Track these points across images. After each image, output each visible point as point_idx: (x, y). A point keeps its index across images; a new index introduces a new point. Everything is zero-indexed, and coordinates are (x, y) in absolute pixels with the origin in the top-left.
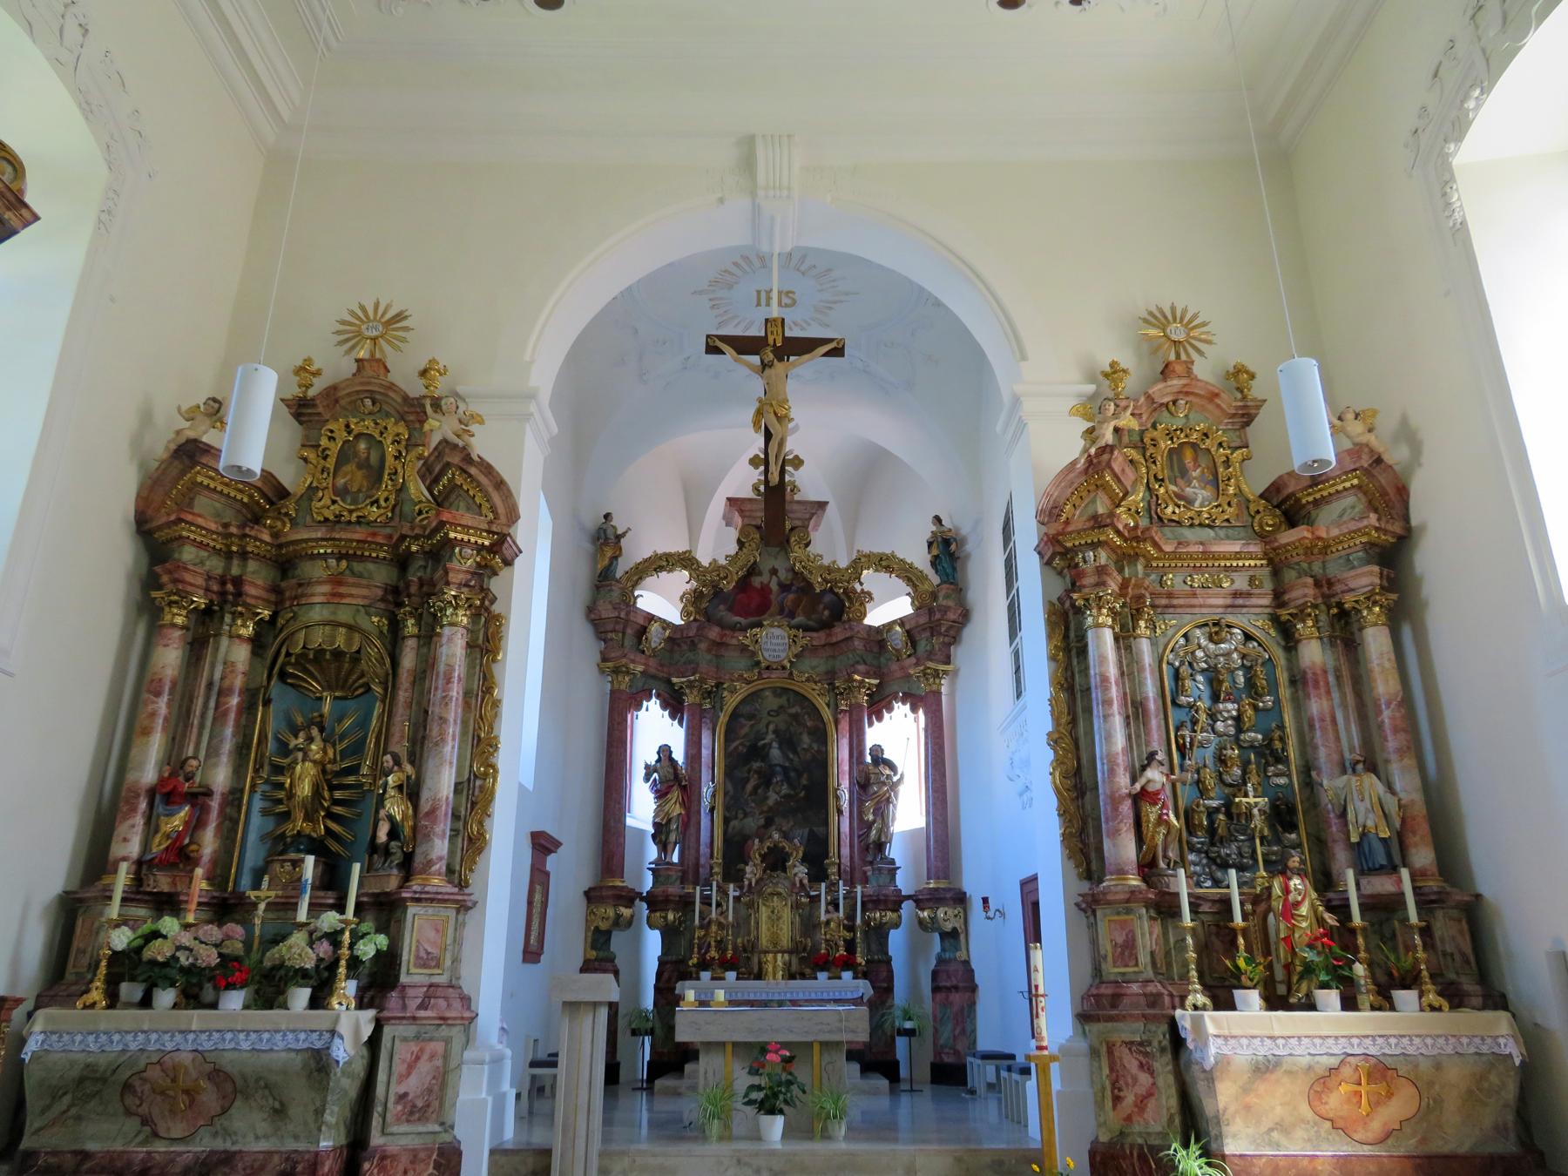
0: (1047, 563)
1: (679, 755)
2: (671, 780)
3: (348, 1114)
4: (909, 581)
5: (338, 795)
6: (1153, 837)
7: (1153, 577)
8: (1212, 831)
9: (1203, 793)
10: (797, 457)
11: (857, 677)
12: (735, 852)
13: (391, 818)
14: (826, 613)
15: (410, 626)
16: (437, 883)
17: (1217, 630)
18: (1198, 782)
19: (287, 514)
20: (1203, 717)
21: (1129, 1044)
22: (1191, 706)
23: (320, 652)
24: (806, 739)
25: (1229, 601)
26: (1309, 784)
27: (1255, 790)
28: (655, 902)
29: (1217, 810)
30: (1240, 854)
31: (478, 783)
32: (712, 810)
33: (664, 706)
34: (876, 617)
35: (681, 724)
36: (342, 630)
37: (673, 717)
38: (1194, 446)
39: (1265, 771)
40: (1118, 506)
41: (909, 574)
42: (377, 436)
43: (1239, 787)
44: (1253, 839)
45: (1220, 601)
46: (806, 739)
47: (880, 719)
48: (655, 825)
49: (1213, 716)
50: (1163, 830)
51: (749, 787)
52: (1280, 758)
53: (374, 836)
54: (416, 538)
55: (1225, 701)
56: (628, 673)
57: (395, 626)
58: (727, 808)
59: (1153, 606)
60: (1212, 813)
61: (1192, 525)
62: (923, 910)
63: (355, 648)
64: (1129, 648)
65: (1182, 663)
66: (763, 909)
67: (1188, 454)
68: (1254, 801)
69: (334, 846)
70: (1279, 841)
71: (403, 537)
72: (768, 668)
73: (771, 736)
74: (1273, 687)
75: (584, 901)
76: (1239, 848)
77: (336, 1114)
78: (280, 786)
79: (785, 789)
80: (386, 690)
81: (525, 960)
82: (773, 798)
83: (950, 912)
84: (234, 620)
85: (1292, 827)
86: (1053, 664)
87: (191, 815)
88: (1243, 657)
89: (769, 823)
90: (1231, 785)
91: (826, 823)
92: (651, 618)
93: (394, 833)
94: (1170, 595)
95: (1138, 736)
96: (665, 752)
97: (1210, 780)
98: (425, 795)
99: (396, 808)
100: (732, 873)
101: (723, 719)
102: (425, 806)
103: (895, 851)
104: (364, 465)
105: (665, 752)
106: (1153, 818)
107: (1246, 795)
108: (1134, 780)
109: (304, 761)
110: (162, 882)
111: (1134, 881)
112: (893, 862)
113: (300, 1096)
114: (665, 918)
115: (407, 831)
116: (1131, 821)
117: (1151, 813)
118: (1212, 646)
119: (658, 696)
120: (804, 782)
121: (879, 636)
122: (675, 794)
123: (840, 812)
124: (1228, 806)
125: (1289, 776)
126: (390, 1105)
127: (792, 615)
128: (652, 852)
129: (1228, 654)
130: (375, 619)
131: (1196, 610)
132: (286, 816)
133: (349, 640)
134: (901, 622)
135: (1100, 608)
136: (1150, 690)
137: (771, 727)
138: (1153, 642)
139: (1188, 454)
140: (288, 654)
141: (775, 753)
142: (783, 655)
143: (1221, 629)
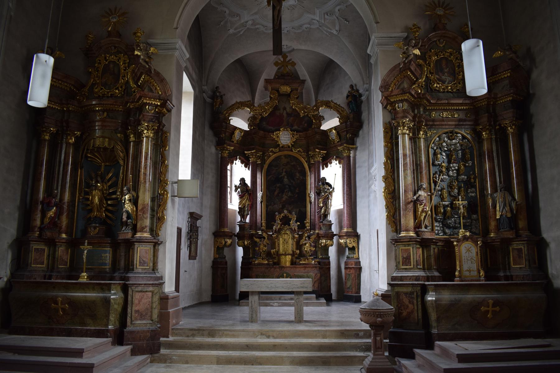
0: (385, 108)
1: (248, 182)
2: (245, 191)
3: (118, 316)
4: (338, 112)
6: (420, 217)
7: (427, 113)
8: (445, 213)
9: (442, 199)
10: (293, 62)
11: (317, 150)
12: (270, 218)
13: (127, 212)
14: (306, 125)
15: (132, 138)
16: (146, 235)
17: (451, 135)
18: (441, 194)
19: (84, 94)
20: (444, 170)
22: (440, 165)
23: (99, 148)
24: (298, 174)
25: (457, 123)
26: (483, 195)
27: (462, 198)
28: (240, 236)
29: (447, 206)
30: (455, 223)
31: (161, 197)
32: (261, 202)
33: (242, 162)
34: (325, 127)
35: (249, 169)
36: (107, 140)
37: (246, 166)
38: (446, 59)
39: (467, 191)
40: (414, 84)
41: (337, 109)
43: (456, 198)
44: (460, 217)
45: (454, 123)
46: (298, 174)
47: (327, 166)
48: (239, 208)
49: (448, 169)
50: (424, 214)
51: (276, 193)
52: (474, 186)
53: (122, 219)
54: (132, 102)
55: (453, 163)
56: (227, 150)
57: (127, 137)
58: (267, 201)
59: (426, 125)
60: (445, 207)
61: (444, 92)
63: (112, 146)
64: (415, 142)
65: (437, 148)
66: (281, 239)
67: (444, 62)
68: (461, 203)
69: (109, 221)
70: (469, 217)
71: (127, 103)
72: (282, 147)
73: (284, 174)
74: (472, 159)
75: (213, 237)
76: (455, 220)
77: (113, 318)
78: (88, 199)
79: (290, 194)
80: (124, 164)
81: (189, 259)
82: (285, 197)
83: (352, 240)
84: (67, 137)
85: (476, 212)
86: (386, 149)
87: (56, 210)
88: (461, 145)
89: (283, 208)
90: (453, 196)
91: (305, 207)
92: (235, 128)
93: (129, 217)
94: (434, 120)
95: (417, 177)
96: (243, 180)
97: (445, 195)
98: (140, 202)
99: (128, 207)
100: (269, 226)
101: (266, 166)
102: (140, 207)
103: (332, 217)
105: (243, 180)
106: (420, 210)
107: (459, 201)
108: (415, 194)
109: (95, 190)
110: (48, 234)
111: (412, 234)
112: (330, 221)
114: (244, 243)
115: (134, 216)
116: (412, 211)
118: (449, 141)
119: (240, 159)
120: (297, 191)
121: (325, 133)
122: (247, 196)
123: (311, 203)
124: (452, 205)
125: (476, 193)
126: (133, 314)
127: (292, 126)
128: (239, 218)
129: (455, 144)
130: (119, 135)
131: (444, 127)
132: (91, 211)
133: (109, 144)
134: (335, 128)
135: (404, 127)
137: (284, 170)
138: (426, 140)
139: (444, 62)
140: (88, 149)
141: (286, 180)
142: (288, 142)
143: (453, 134)
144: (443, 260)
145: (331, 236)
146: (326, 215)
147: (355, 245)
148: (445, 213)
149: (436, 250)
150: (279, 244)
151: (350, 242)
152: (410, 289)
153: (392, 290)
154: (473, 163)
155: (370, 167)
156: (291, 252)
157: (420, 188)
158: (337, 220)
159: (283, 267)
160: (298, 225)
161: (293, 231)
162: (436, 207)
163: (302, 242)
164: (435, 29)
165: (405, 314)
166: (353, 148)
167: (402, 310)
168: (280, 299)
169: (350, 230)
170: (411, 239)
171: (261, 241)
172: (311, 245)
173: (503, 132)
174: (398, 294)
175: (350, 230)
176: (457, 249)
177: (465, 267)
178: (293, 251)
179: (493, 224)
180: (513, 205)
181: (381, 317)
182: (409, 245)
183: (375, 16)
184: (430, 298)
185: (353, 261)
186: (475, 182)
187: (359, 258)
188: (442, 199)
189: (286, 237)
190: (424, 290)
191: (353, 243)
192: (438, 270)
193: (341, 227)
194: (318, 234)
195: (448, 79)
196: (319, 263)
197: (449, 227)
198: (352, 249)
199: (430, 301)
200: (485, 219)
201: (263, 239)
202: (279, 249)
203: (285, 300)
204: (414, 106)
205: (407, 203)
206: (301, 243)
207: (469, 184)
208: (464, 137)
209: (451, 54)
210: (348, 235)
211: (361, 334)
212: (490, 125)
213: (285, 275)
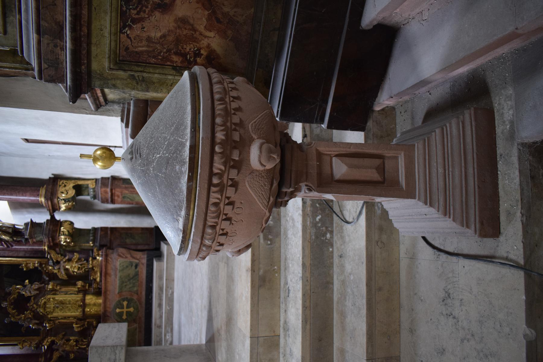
62: (60, 208)
66: (55, 314)
83: (62, 189)
103: (19, 220)
112: (26, 224)
145: (54, 224)
146: (14, 231)
147: (72, 185)
150: (65, 318)
151: (65, 193)
156: (80, 296)
158: (30, 210)
159: (105, 311)
160: (31, 283)
161: (42, 292)
163: (62, 275)
167: (197, 54)
168: (160, 327)
169: (43, 191)
171: (57, 350)
172: (69, 260)
175: (43, 191)
178: (79, 292)
181: (243, 145)
185: (100, 191)
187: (96, 180)
189: (50, 306)
191: (67, 188)
193: (36, 206)
194: (49, 247)
196: (101, 247)
198: (79, 189)
201: (54, 347)
202: (75, 317)
203: (161, 317)
206: (65, 277)
210: (51, 196)
213: (118, 310)
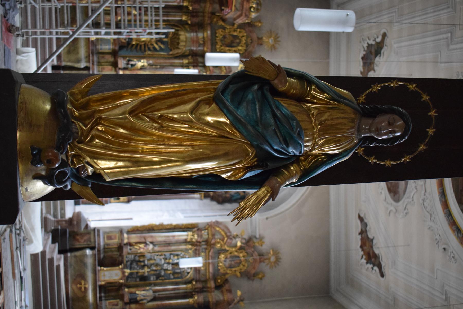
5: (143, 46)
20: (167, 261)
21: (90, 238)
22: (170, 259)
23: (179, 39)
26: (150, 285)
29: (144, 263)
42: (241, 44)
60: (144, 261)
70: (138, 277)
74: (175, 278)
77: (69, 64)
93: (132, 65)
97: (152, 262)
104: (232, 42)
111: (126, 241)
113: (73, 57)
117: (142, 246)
133: (181, 46)
136: (173, 248)
140: (178, 30)
144: (110, 258)
148: (140, 261)
149: (116, 256)
152: (92, 240)
153: (91, 230)
154: (172, 279)
155: (183, 211)
157: (154, 245)
162: (144, 256)
164: (261, 255)
165: (78, 237)
166: (201, 196)
170: (122, 240)
173: (191, 296)
174: (89, 233)
176: (117, 268)
177: (107, 273)
179: (133, 290)
180: (145, 301)
182: (119, 239)
183: (272, 217)
184: (88, 252)
186: (160, 280)
188: (149, 260)
190: (92, 248)
192: (104, 257)
195: (227, 264)
197: (131, 264)
199: (86, 252)
200: (137, 286)
204: (207, 242)
205: (145, 238)
207: (158, 276)
208: (188, 273)
209: (244, 266)
211: (63, 212)
212: (195, 289)
